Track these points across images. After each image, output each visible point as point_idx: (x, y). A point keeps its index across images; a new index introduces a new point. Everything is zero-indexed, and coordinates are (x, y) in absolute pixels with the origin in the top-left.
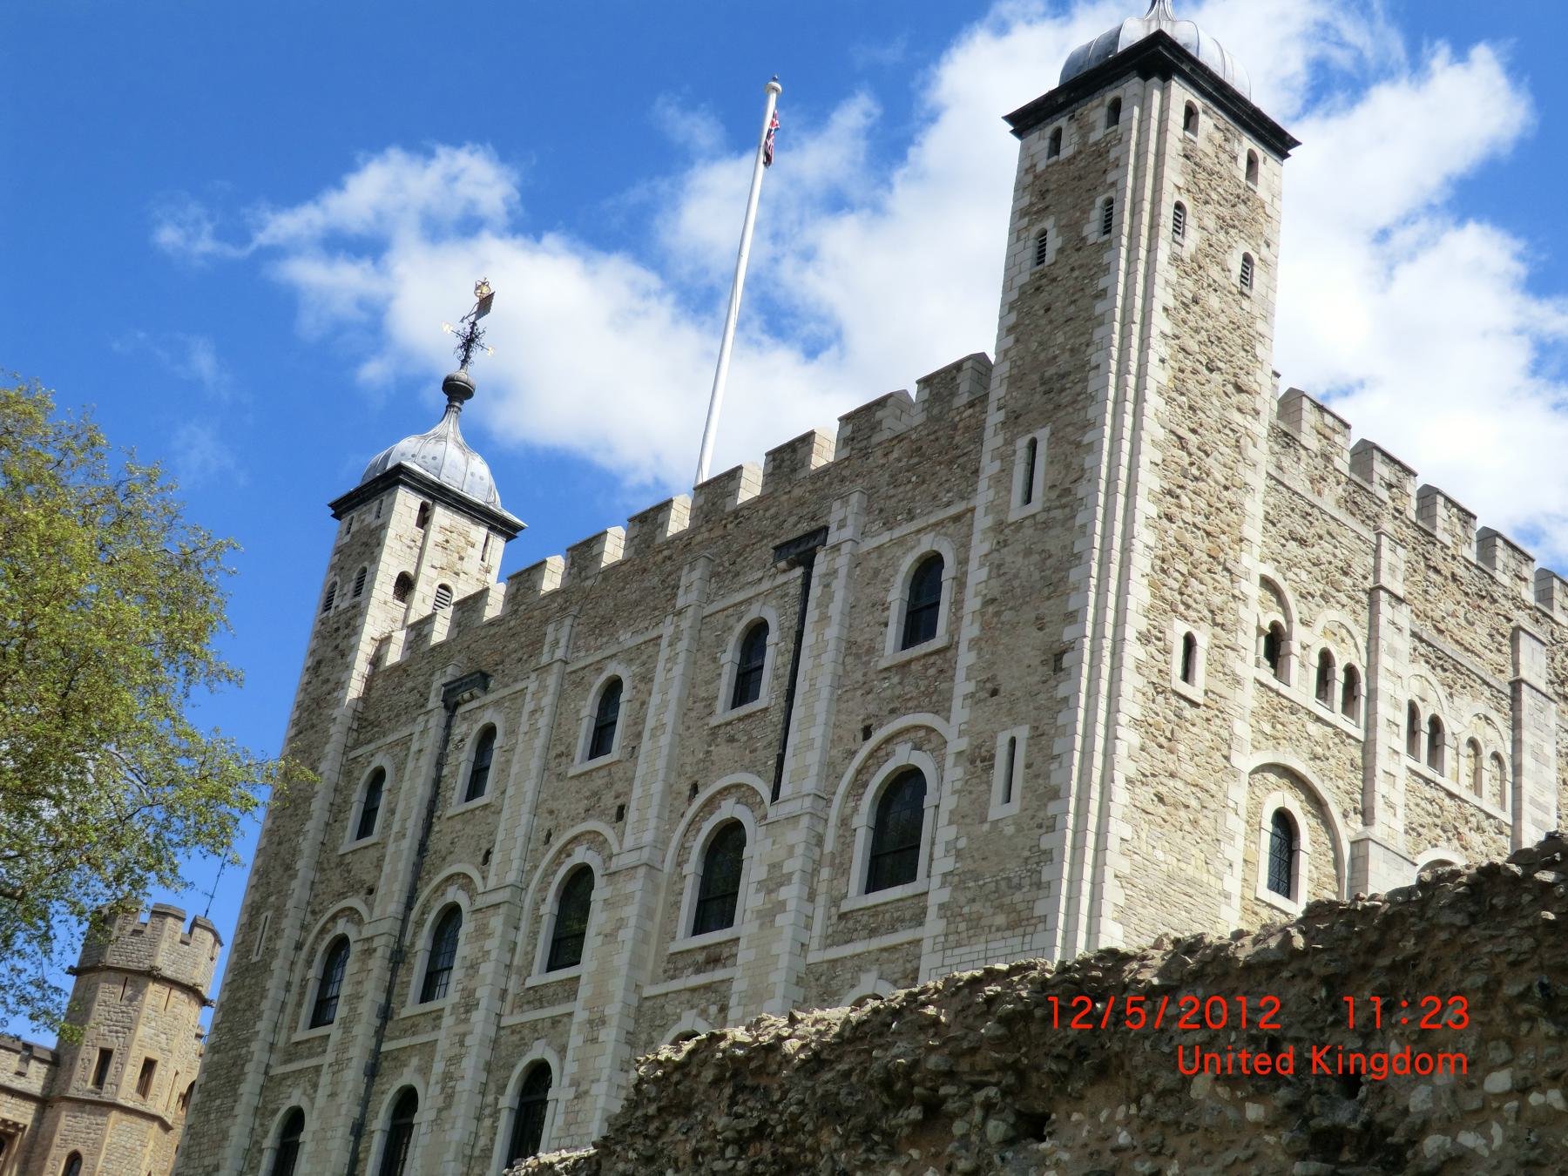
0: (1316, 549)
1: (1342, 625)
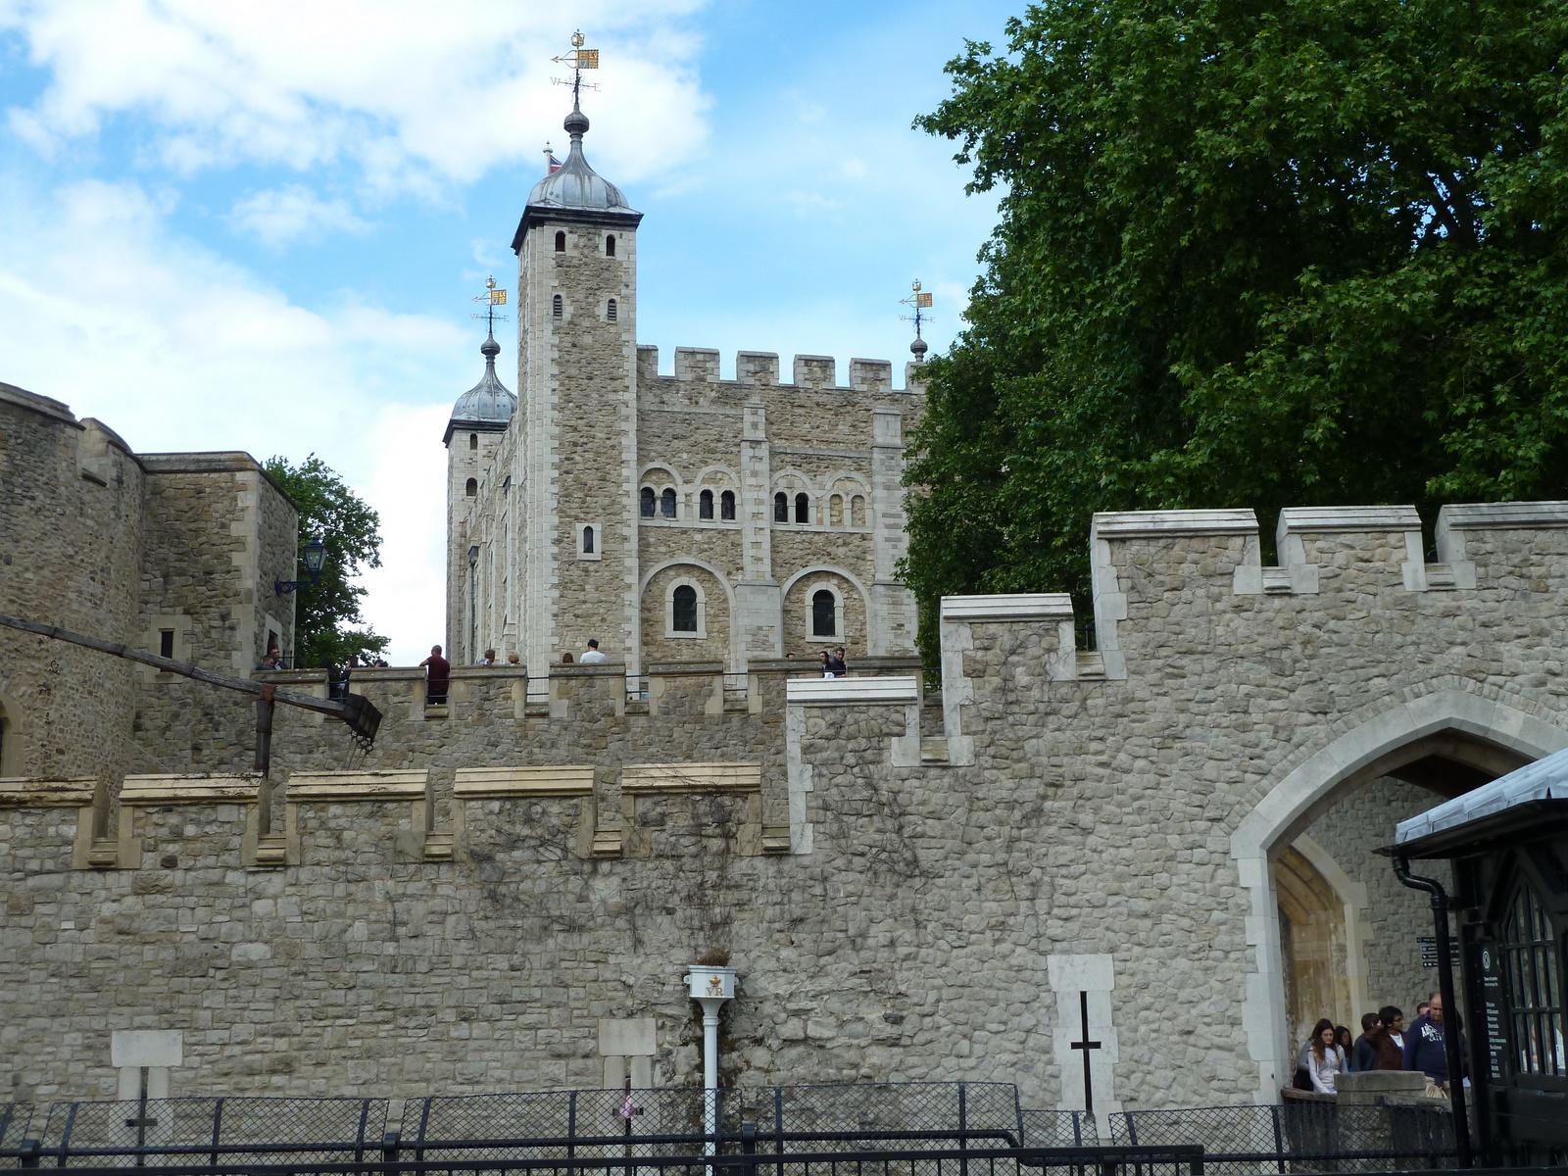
1: (717, 472)
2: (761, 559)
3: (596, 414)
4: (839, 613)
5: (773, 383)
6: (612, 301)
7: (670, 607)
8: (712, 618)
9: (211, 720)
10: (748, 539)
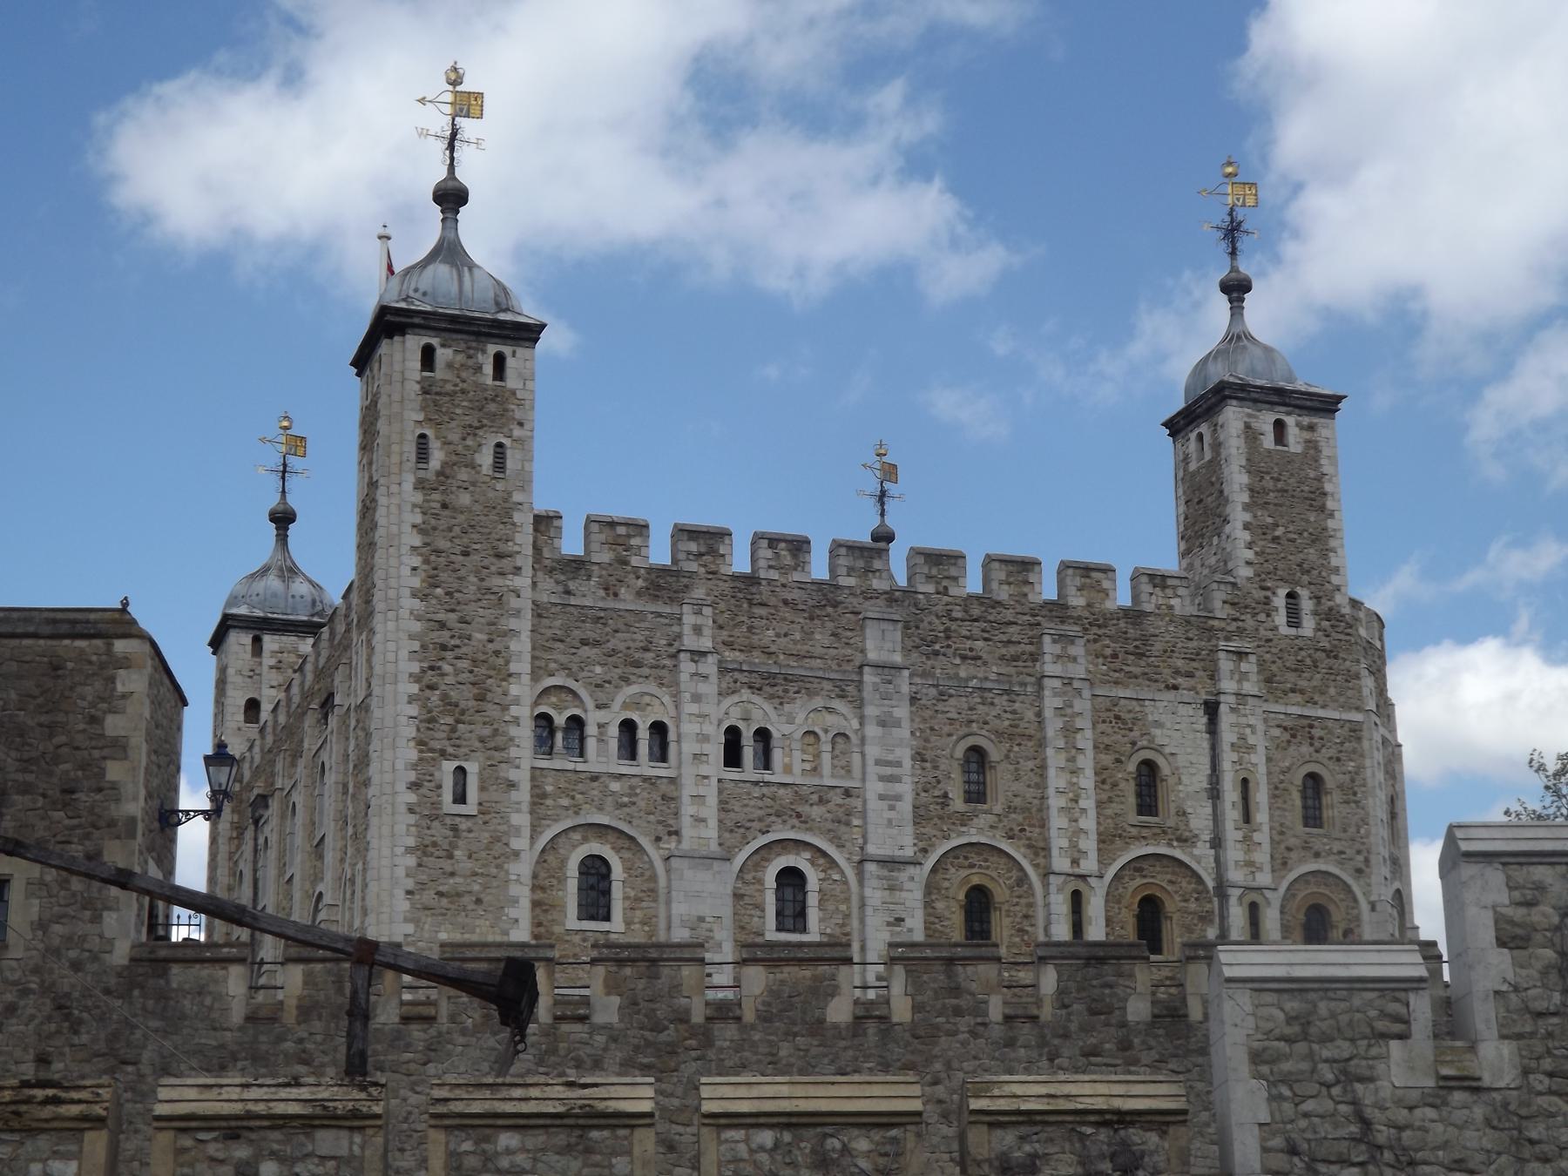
0: (610, 645)
2: (703, 820)
3: (473, 606)
4: (812, 900)
5: (724, 570)
6: (499, 445)
7: (572, 885)
8: (633, 903)
9: (67, 1017)
10: (688, 788)
